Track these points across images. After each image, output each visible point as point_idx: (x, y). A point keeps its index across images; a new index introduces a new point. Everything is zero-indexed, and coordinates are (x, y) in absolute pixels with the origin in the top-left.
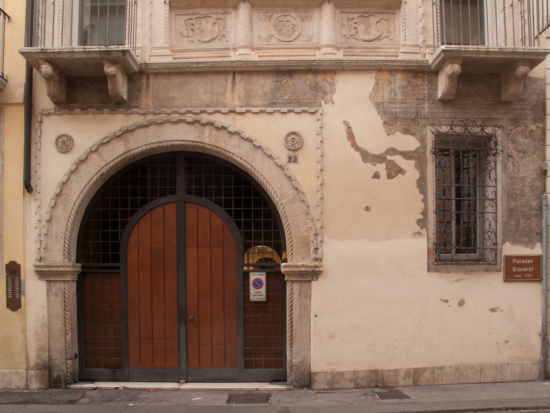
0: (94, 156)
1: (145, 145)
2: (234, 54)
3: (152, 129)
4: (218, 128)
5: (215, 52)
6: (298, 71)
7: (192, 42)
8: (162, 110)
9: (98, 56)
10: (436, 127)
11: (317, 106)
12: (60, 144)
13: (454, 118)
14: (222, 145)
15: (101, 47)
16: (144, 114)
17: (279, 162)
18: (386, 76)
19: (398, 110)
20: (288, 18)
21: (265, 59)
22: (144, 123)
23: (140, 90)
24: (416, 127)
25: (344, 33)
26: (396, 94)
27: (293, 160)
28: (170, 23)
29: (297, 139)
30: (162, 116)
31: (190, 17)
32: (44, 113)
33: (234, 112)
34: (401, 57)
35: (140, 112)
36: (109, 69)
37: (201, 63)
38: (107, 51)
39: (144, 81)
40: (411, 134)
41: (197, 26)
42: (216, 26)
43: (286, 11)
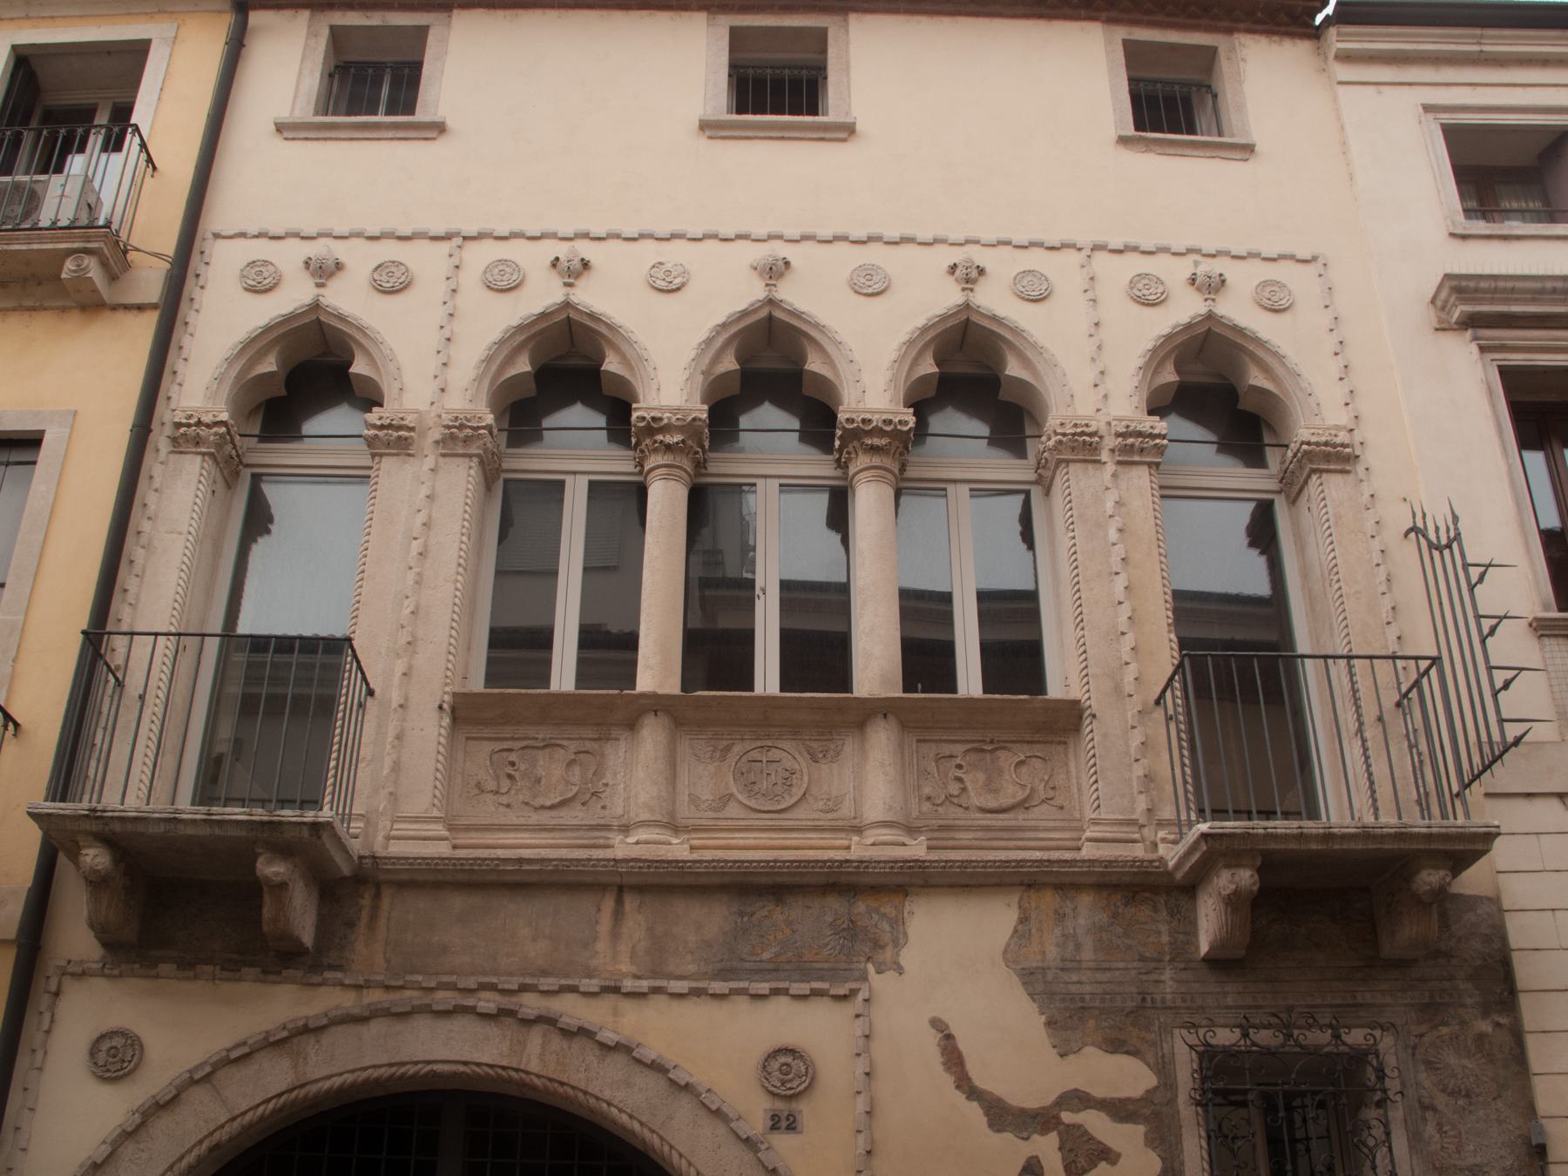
0: (198, 1095)
1: (353, 1071)
2: (623, 842)
3: (377, 1027)
4: (567, 1033)
5: (569, 834)
6: (799, 886)
7: (508, 806)
8: (408, 978)
10: (1201, 1032)
11: (856, 980)
13: (1249, 1007)
14: (577, 1078)
16: (358, 987)
17: (745, 1130)
18: (1049, 900)
19: (1088, 988)
20: (775, 754)
21: (708, 855)
22: (357, 1011)
23: (351, 925)
24: (1143, 1034)
25: (927, 790)
26: (1078, 947)
27: (784, 1124)
28: (451, 758)
29: (798, 1066)
30: (408, 993)
31: (506, 745)
33: (616, 990)
34: (1089, 851)
35: (347, 982)
37: (530, 861)
39: (366, 901)
40: (1128, 1053)
41: (523, 767)
42: (577, 770)
43: (769, 737)
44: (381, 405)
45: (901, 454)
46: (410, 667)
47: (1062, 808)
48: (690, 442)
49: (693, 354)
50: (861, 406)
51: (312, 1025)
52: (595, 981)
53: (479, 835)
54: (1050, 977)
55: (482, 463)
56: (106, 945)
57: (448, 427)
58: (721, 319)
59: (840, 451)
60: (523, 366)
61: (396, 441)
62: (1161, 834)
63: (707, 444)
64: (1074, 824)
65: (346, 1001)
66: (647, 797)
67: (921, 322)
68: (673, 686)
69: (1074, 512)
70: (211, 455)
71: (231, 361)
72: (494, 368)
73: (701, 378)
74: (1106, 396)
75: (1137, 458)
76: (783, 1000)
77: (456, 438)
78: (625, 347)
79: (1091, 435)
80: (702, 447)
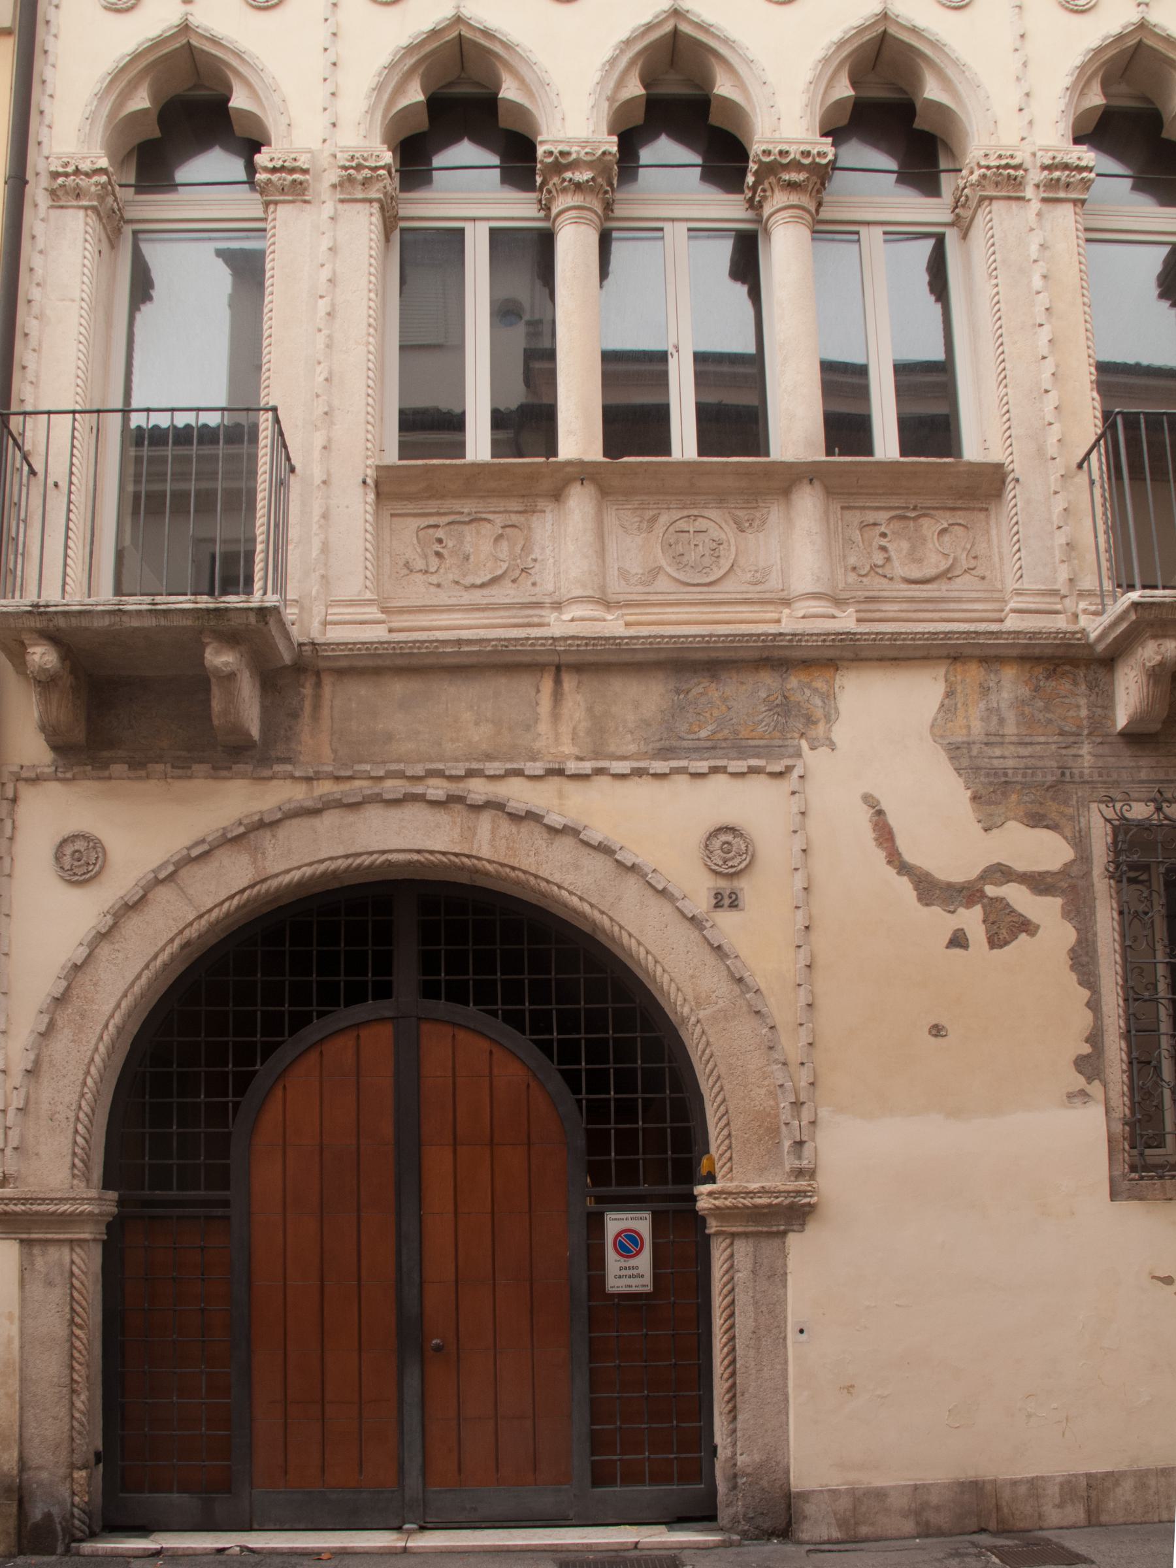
0: (164, 894)
1: (311, 864)
2: (558, 619)
3: (330, 819)
4: (515, 818)
5: (502, 613)
6: (734, 662)
7: (439, 586)
8: (357, 767)
9: (189, 623)
10: (1118, 805)
11: (790, 757)
12: (67, 861)
13: (1162, 782)
14: (527, 862)
15: (199, 598)
16: (308, 779)
17: (690, 909)
18: (974, 673)
19: (1010, 763)
20: (702, 524)
21: (645, 631)
22: (309, 804)
23: (295, 715)
24: (1062, 808)
25: (852, 560)
26: (1002, 721)
27: (727, 902)
28: (378, 536)
29: (739, 844)
30: (357, 783)
31: (432, 521)
32: (24, 774)
33: (560, 772)
34: (1012, 623)
35: (297, 774)
36: (220, 658)
37: (469, 642)
38: (217, 610)
39: (308, 690)
40: (1047, 827)
41: (450, 544)
42: (504, 544)
43: (694, 505)
44: (269, 145)
45: (819, 192)
46: (329, 440)
47: (983, 578)
48: (600, 180)
49: (597, 76)
50: (777, 135)
51: (267, 820)
52: (538, 764)
53: (411, 617)
54: (975, 752)
55: (382, 208)
56: (55, 748)
57: (345, 168)
58: (624, 35)
59: (754, 188)
60: (415, 95)
61: (293, 186)
62: (1083, 605)
63: (615, 182)
64: (996, 595)
65: (297, 794)
66: (578, 568)
67: (836, 35)
68: (594, 452)
69: (997, 256)
70: (94, 208)
71: (101, 97)
72: (386, 97)
73: (606, 105)
74: (1031, 122)
75: (1062, 195)
76: (721, 778)
77: (353, 179)
78: (523, 70)
79: (1017, 167)
80: (611, 185)
